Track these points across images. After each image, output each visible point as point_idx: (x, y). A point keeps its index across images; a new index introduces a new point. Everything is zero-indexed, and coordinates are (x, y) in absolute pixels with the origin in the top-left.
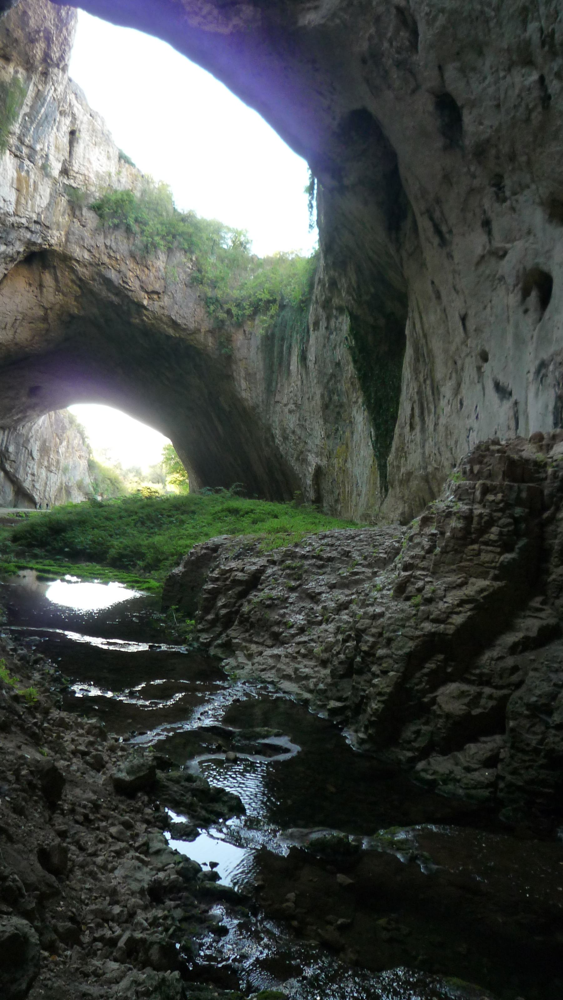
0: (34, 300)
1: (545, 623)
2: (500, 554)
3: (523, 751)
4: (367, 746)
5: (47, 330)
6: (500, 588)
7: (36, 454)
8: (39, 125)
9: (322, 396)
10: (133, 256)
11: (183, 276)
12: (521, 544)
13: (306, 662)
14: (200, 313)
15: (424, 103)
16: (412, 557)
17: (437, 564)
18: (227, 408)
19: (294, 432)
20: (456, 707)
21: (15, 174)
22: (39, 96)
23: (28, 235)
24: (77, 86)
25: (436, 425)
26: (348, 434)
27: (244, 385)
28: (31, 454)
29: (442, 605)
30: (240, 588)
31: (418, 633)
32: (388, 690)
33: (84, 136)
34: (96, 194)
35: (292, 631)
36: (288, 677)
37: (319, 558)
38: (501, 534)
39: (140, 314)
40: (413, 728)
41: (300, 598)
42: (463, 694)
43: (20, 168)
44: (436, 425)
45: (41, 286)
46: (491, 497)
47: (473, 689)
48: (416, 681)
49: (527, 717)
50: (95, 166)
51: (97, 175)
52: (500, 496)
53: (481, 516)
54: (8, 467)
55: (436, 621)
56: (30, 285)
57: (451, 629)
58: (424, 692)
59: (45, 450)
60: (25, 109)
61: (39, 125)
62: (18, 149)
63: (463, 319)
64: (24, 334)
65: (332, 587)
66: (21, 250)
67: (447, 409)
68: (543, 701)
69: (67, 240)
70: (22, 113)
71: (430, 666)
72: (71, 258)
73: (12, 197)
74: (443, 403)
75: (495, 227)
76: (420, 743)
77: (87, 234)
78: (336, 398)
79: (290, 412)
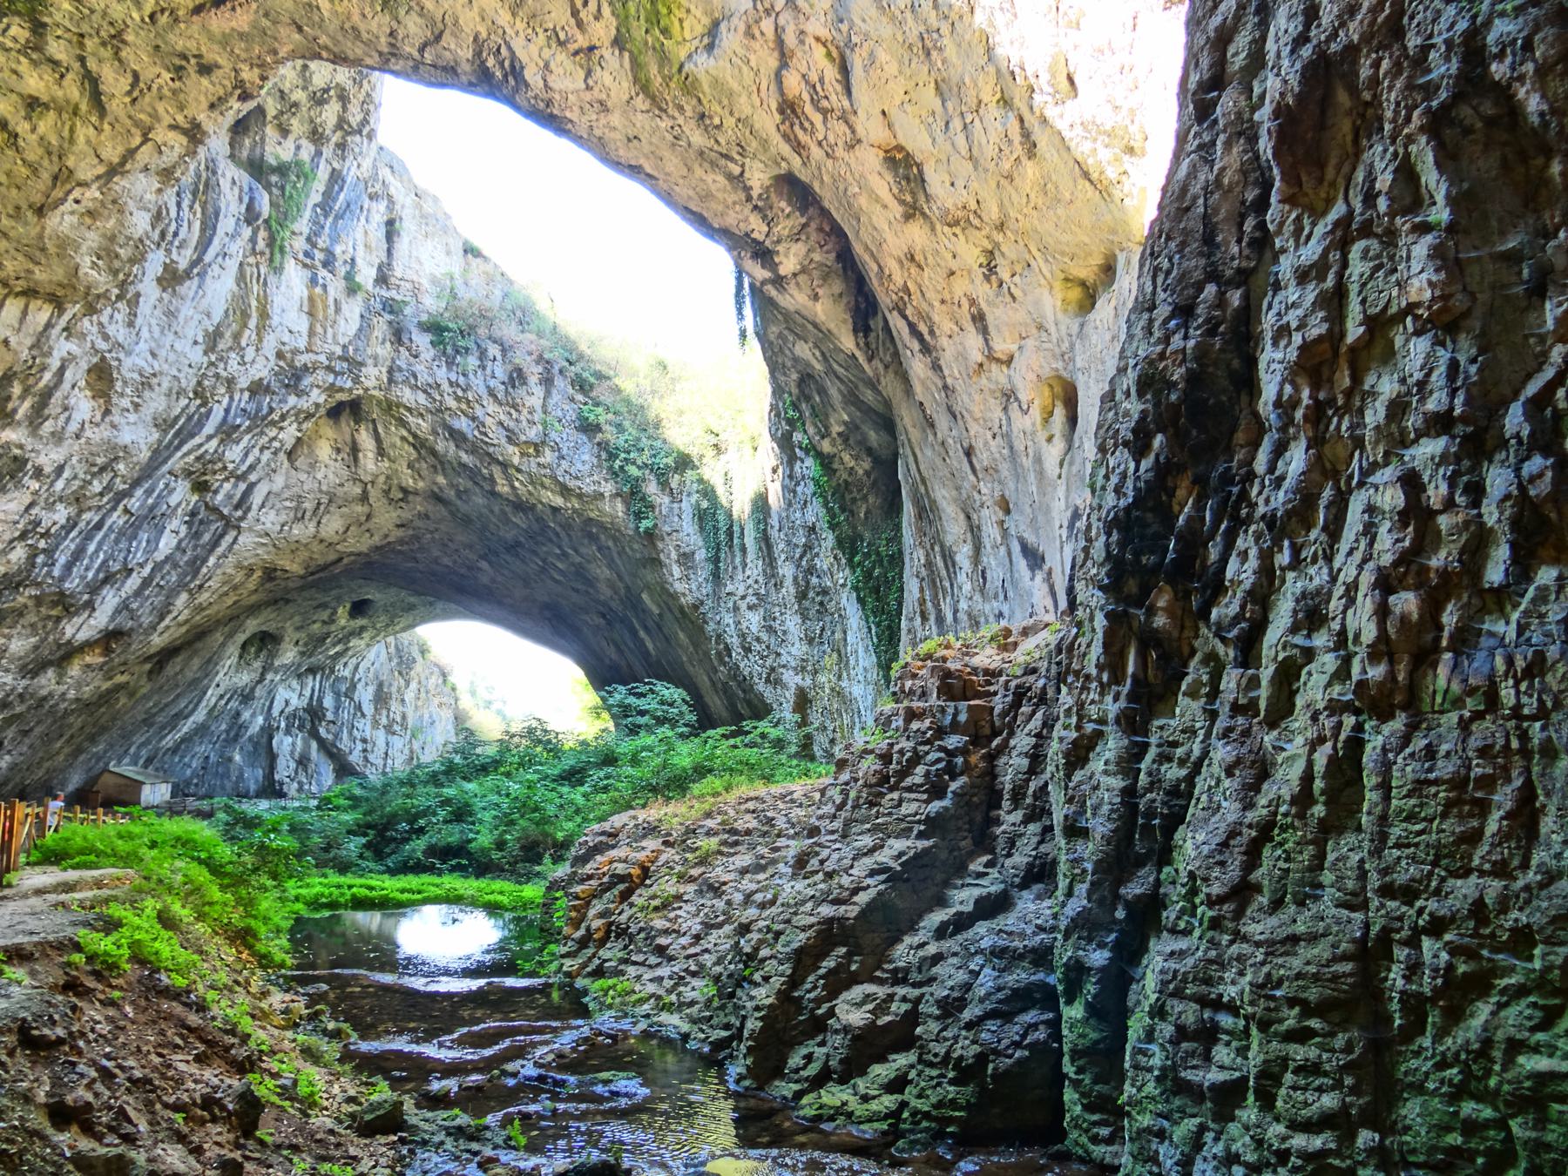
0: (345, 473)
1: (984, 891)
2: (927, 802)
3: (931, 1065)
4: (747, 1083)
5: (369, 517)
6: (926, 851)
7: (368, 709)
8: (337, 218)
9: (795, 578)
12: (954, 786)
13: (696, 982)
15: (869, 161)
16: (820, 818)
17: (847, 824)
18: (656, 611)
19: (758, 639)
20: (856, 1018)
21: (306, 293)
22: (336, 177)
23: (331, 378)
24: (391, 154)
25: (956, 611)
26: (838, 635)
27: (677, 571)
28: (359, 707)
29: (846, 881)
30: (621, 887)
31: (813, 920)
32: (770, 1001)
33: (408, 227)
34: (432, 304)
35: (684, 941)
36: (669, 1008)
37: (733, 832)
38: (927, 774)
40: (804, 1051)
41: (700, 892)
42: (868, 998)
43: (313, 281)
44: (956, 611)
45: (355, 449)
46: (915, 725)
47: (881, 991)
48: (808, 986)
49: (937, 1018)
50: (426, 266)
51: (434, 281)
52: (927, 723)
53: (902, 752)
54: (322, 731)
55: (837, 902)
56: (338, 451)
57: (852, 911)
58: (818, 1002)
60: (316, 198)
61: (337, 218)
62: (307, 254)
63: (969, 452)
65: (744, 871)
66: (321, 400)
67: (967, 587)
68: (956, 994)
69: (391, 381)
70: (310, 204)
71: (829, 963)
72: (399, 405)
73: (303, 325)
74: (962, 578)
75: (990, 319)
76: (813, 1070)
78: (814, 580)
79: (750, 608)
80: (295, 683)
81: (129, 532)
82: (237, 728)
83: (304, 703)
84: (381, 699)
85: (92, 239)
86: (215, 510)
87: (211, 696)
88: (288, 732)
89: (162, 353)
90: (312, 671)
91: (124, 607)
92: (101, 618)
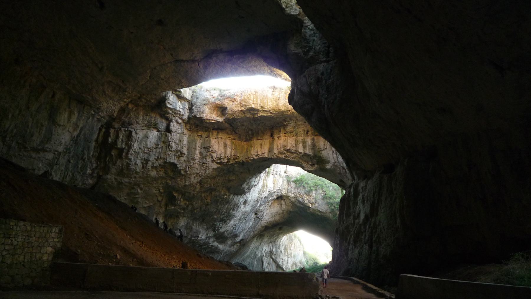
7: (283, 251)
10: (306, 194)
11: (321, 197)
14: (327, 207)
39: (309, 209)
45: (281, 205)
54: (273, 257)
59: (286, 249)
64: (277, 218)
73: (272, 185)
77: (293, 189)
80: (267, 245)
81: (246, 223)
82: (256, 255)
83: (269, 250)
84: (286, 249)
85: (247, 187)
86: (258, 218)
87: (251, 248)
88: (266, 257)
89: (253, 196)
90: (271, 242)
91: (244, 235)
92: (241, 238)
